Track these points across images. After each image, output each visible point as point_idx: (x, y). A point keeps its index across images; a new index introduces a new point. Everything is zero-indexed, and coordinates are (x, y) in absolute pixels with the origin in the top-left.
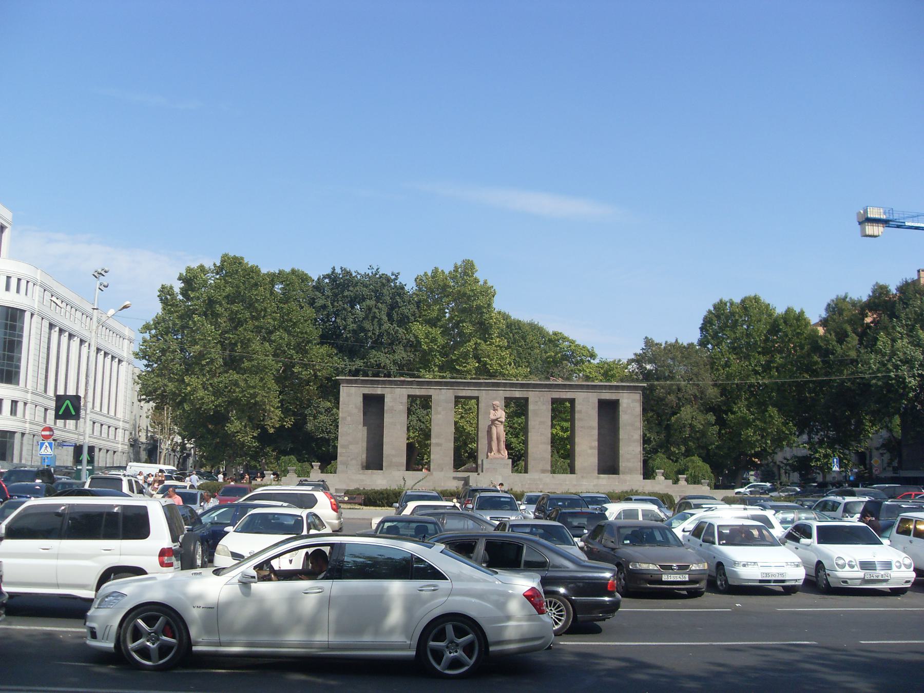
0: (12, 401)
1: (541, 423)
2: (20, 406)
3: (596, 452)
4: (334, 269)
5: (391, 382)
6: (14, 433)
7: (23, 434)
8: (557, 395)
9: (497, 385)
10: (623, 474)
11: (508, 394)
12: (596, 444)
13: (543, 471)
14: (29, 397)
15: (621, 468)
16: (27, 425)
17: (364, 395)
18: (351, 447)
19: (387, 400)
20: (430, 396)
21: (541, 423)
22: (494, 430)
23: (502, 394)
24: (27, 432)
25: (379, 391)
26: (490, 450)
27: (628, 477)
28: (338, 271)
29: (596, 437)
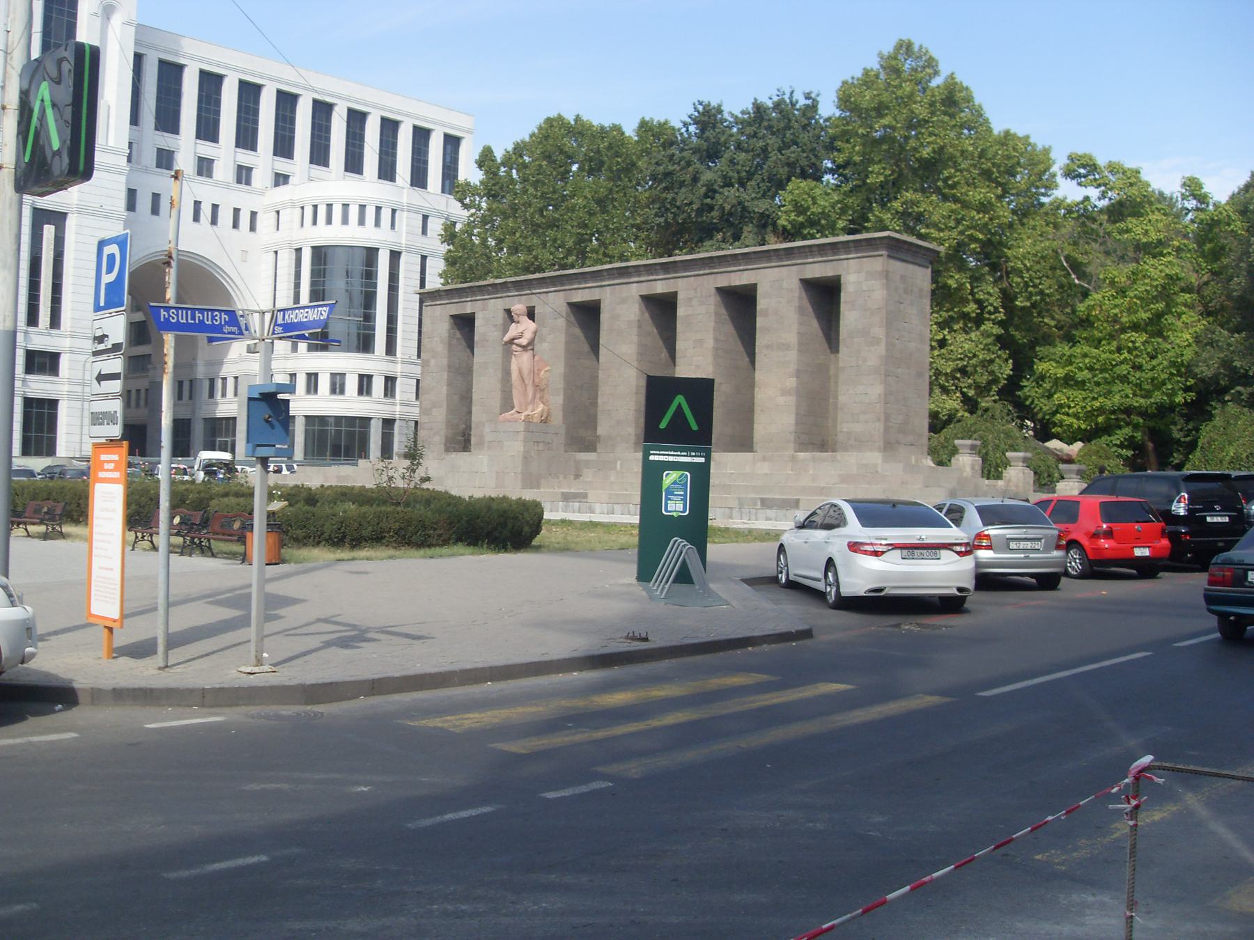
0: (361, 377)
1: (699, 343)
2: (378, 385)
5: (482, 289)
6: (370, 419)
7: (388, 423)
9: (623, 272)
11: (646, 289)
14: (397, 369)
15: (841, 438)
16: (398, 408)
19: (477, 323)
21: (699, 343)
23: (635, 290)
24: (397, 417)
25: (468, 309)
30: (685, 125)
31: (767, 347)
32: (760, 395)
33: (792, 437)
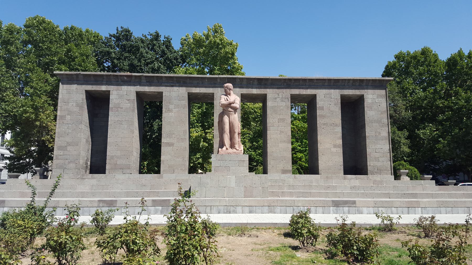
3: (340, 150)
4: (117, 29)
8: (296, 92)
10: (373, 173)
11: (245, 91)
12: (340, 142)
13: (284, 172)
17: (87, 92)
18: (69, 148)
19: (111, 97)
20: (162, 93)
22: (226, 119)
25: (104, 88)
26: (222, 145)
27: (377, 178)
28: (120, 29)
29: (340, 135)
30: (110, 35)
31: (324, 124)
32: (321, 147)
33: (342, 168)
